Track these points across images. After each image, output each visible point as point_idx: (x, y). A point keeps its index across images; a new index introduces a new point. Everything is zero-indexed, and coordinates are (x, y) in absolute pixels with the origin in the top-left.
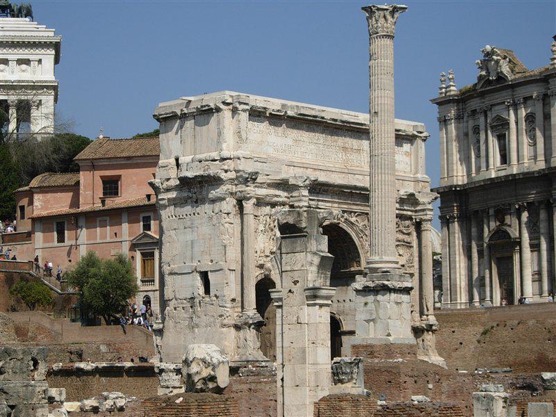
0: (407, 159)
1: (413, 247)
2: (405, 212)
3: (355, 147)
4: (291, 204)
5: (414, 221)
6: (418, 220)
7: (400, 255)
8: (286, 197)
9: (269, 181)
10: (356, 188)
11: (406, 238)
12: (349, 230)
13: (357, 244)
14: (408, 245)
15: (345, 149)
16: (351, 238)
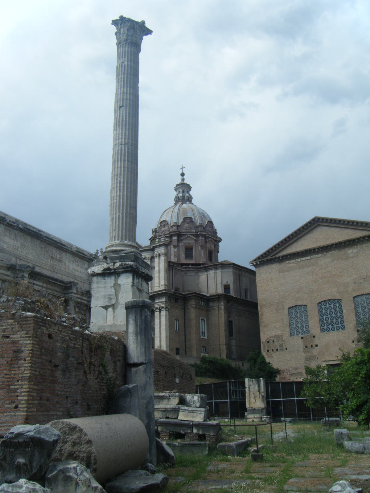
4: (16, 282)
15: (52, 258)
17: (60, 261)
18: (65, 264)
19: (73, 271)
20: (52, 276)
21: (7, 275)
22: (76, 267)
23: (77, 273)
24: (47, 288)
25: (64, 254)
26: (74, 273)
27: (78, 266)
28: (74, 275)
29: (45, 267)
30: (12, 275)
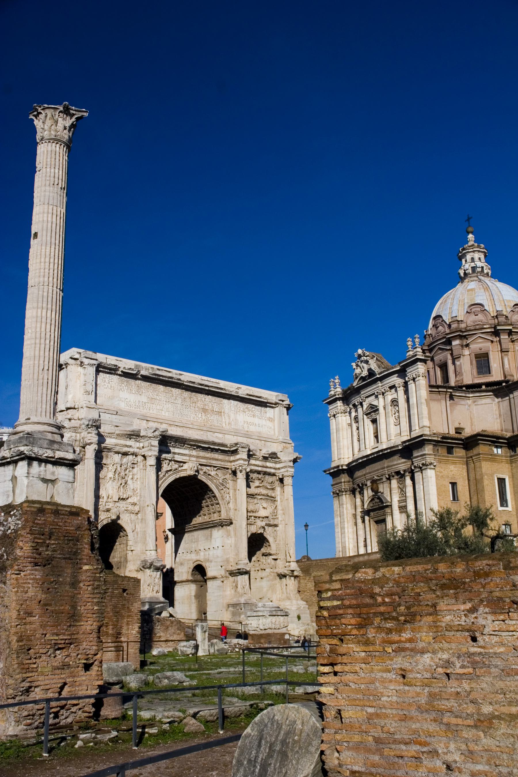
0: (270, 424)
1: (277, 501)
2: (268, 470)
3: (216, 409)
4: (143, 454)
5: (278, 478)
6: (281, 477)
7: (264, 508)
8: (138, 448)
9: (117, 432)
10: (214, 444)
11: (270, 493)
12: (209, 483)
13: (217, 495)
14: (273, 499)
15: (205, 410)
16: (211, 490)
17: (219, 413)
18: (229, 417)
19: (245, 425)
20: (204, 438)
21: (127, 446)
22: (250, 419)
23: (252, 429)
24: (198, 457)
25: (225, 401)
26: (246, 429)
27: (254, 416)
28: (247, 431)
29: (191, 426)
30: (138, 444)
